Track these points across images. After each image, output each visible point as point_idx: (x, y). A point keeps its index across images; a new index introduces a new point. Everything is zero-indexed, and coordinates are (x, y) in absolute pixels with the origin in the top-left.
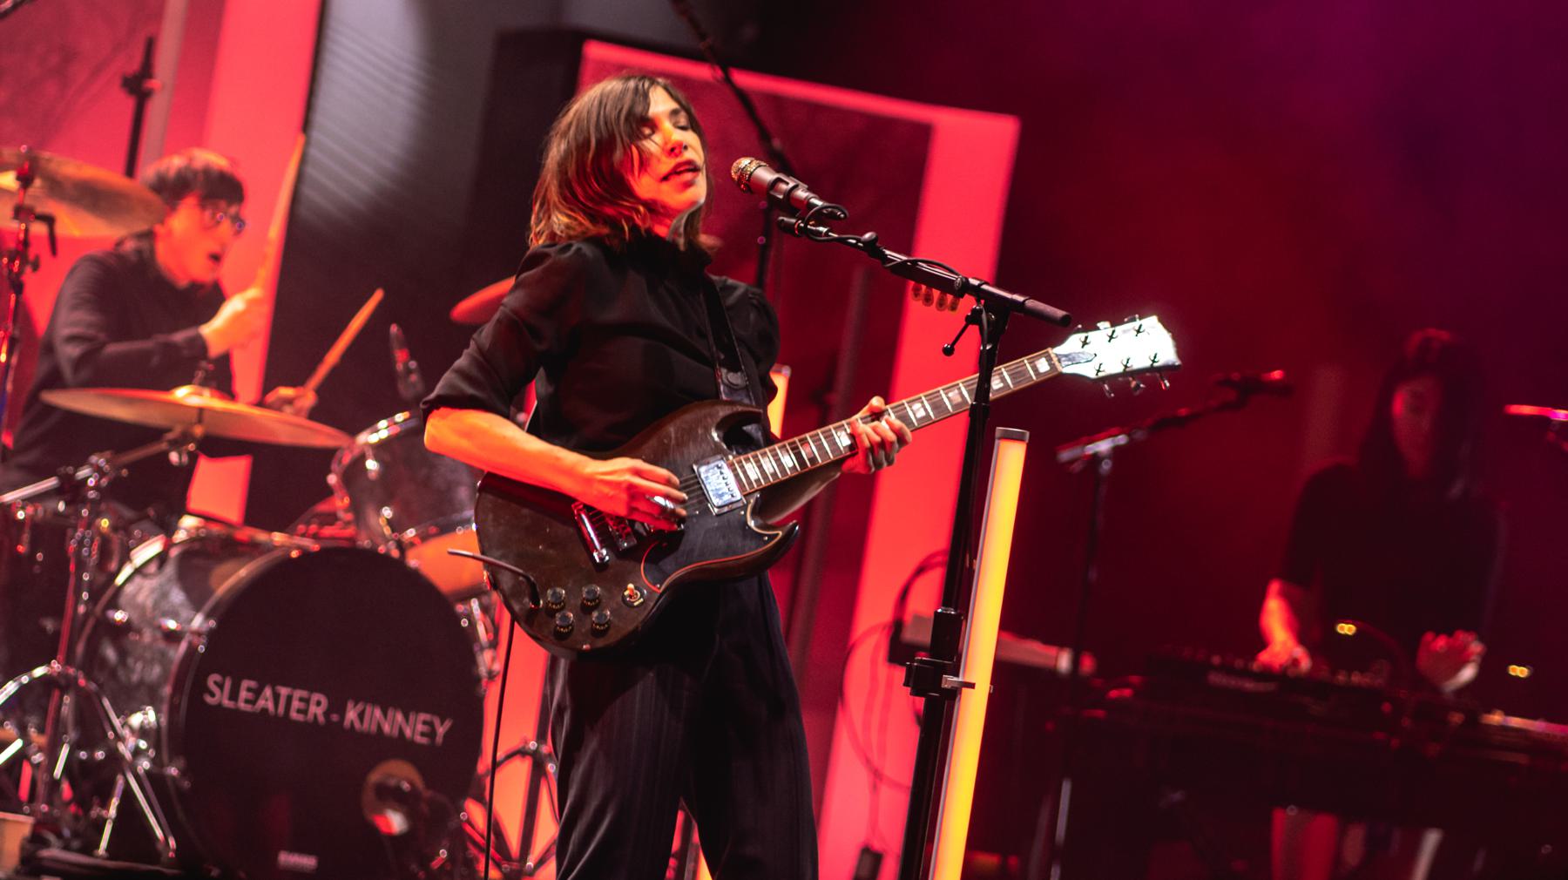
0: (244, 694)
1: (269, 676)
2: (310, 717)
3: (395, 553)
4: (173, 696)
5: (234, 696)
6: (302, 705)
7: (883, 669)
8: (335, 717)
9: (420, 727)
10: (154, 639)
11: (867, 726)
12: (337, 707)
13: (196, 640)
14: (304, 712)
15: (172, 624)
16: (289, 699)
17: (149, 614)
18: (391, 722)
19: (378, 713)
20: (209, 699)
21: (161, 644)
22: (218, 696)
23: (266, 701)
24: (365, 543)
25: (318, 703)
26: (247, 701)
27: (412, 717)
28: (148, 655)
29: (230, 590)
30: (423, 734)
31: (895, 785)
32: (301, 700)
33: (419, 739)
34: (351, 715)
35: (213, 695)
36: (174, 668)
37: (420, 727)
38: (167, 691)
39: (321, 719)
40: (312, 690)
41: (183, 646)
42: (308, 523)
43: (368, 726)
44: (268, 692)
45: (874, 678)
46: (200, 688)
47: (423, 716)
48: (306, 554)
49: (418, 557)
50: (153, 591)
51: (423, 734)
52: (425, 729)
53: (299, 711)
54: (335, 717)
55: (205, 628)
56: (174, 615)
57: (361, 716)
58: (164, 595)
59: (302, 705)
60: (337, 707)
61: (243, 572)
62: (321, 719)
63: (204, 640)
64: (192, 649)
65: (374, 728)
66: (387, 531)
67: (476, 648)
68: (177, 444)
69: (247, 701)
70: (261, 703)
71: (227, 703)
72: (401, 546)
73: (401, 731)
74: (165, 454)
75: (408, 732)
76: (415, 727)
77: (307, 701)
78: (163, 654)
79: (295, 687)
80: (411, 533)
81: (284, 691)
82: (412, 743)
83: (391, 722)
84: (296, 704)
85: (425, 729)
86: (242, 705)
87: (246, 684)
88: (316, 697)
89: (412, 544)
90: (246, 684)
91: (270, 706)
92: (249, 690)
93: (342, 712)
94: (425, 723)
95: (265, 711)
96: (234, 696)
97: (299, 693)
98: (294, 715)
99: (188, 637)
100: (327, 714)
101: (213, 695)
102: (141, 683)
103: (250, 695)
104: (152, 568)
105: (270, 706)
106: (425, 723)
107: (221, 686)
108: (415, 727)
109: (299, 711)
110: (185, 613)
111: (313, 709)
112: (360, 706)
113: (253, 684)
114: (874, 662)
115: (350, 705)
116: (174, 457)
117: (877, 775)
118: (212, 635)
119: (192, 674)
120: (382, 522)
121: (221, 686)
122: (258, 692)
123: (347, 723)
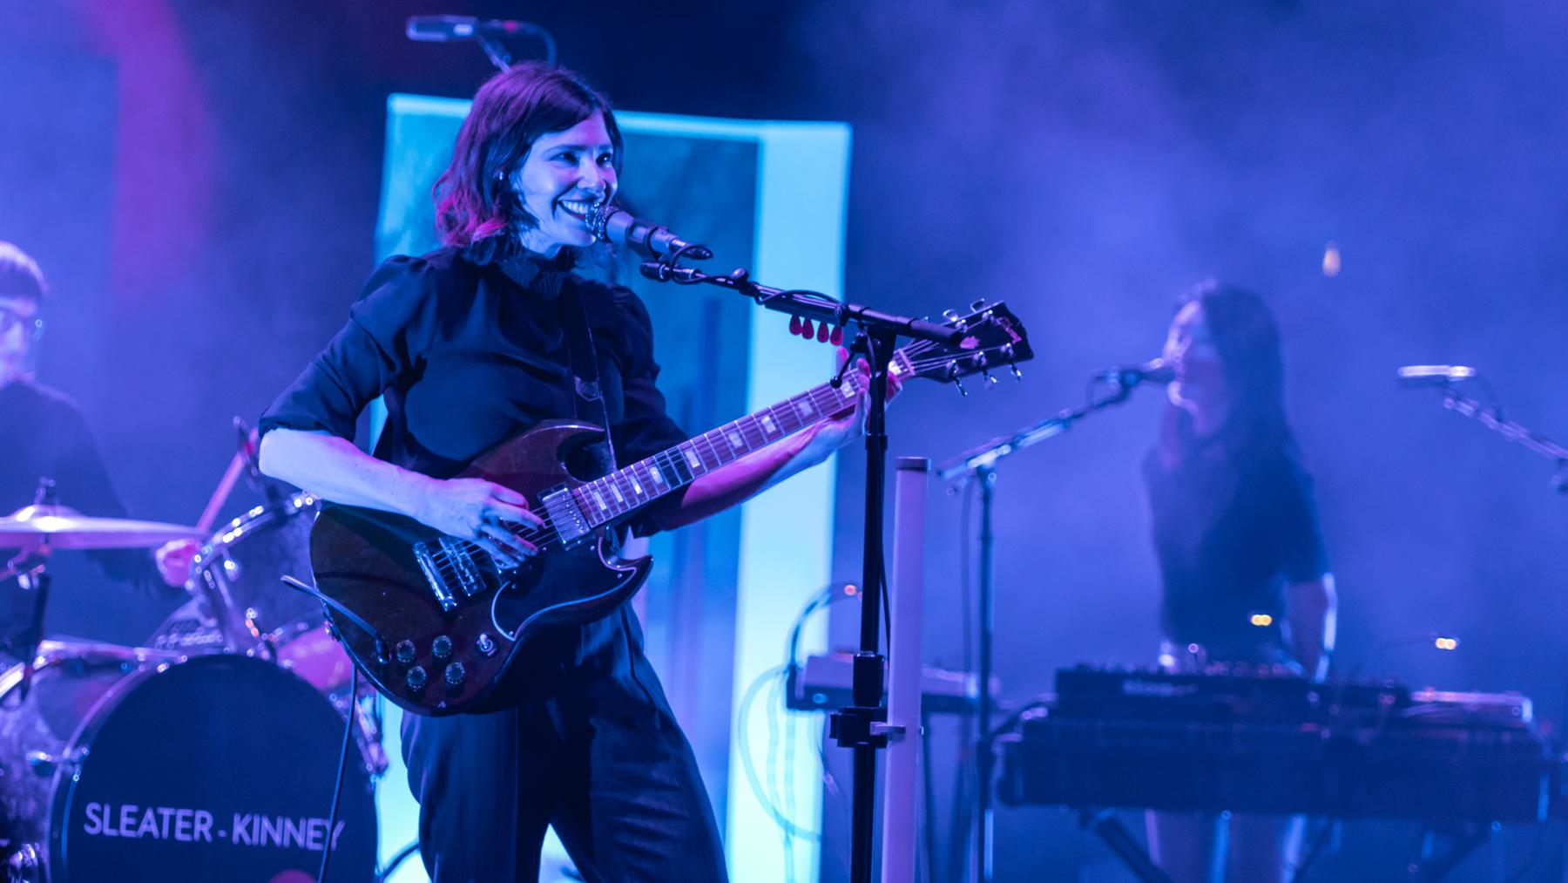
0: (124, 820)
1: (147, 800)
2: (197, 836)
3: (265, 655)
4: (52, 830)
5: (115, 823)
6: (187, 825)
7: (783, 716)
8: (222, 834)
9: (312, 834)
10: (25, 774)
11: (771, 779)
12: (222, 822)
13: (69, 768)
14: (190, 831)
15: (42, 756)
16: (173, 819)
17: (16, 750)
18: (281, 832)
19: (266, 823)
20: (88, 829)
21: (34, 779)
22: (100, 826)
23: (149, 825)
24: (231, 648)
25: (203, 821)
26: (129, 827)
27: (302, 823)
28: (21, 790)
29: (99, 714)
30: (315, 840)
31: (804, 835)
32: (185, 819)
33: (312, 846)
34: (239, 829)
35: (93, 825)
36: (50, 801)
37: (312, 834)
38: (46, 825)
39: (208, 837)
40: (195, 808)
41: (57, 776)
42: (168, 633)
43: (258, 838)
44: (149, 814)
45: (774, 727)
46: (79, 819)
47: (313, 822)
48: (174, 668)
49: (290, 657)
50: (18, 723)
51: (315, 840)
52: (318, 834)
53: (184, 831)
54: (222, 834)
55: (76, 756)
56: (44, 747)
57: (249, 828)
58: (30, 727)
59: (187, 825)
60: (222, 822)
61: (110, 694)
62: (208, 837)
63: (78, 769)
64: (66, 779)
65: (264, 840)
66: (254, 632)
67: (361, 744)
68: (25, 568)
69: (129, 827)
70: (144, 827)
71: (108, 831)
72: (270, 646)
73: (292, 839)
74: (15, 579)
75: (300, 841)
76: (306, 834)
77: (191, 820)
78: (37, 789)
79: (177, 806)
80: (279, 632)
81: (166, 812)
82: (305, 849)
83: (281, 832)
84: (180, 824)
85: (318, 834)
86: (124, 832)
87: (125, 809)
88: (200, 814)
89: (282, 643)
90: (125, 809)
91: (154, 829)
92: (129, 815)
93: (230, 830)
94: (316, 828)
95: (148, 834)
96: (115, 823)
97: (181, 813)
98: (179, 836)
99: (60, 767)
100: (213, 831)
101: (93, 825)
102: (18, 817)
103: (132, 821)
104: (15, 700)
105: (154, 829)
106: (316, 828)
107: (100, 815)
108: (306, 834)
109: (184, 831)
110: (54, 743)
111: (198, 827)
112: (247, 819)
113: (134, 809)
114: (771, 712)
115: (237, 818)
116: (24, 581)
117: (789, 828)
118: (87, 764)
119: (73, 800)
120: (249, 624)
121: (100, 815)
122: (139, 816)
123: (235, 839)
